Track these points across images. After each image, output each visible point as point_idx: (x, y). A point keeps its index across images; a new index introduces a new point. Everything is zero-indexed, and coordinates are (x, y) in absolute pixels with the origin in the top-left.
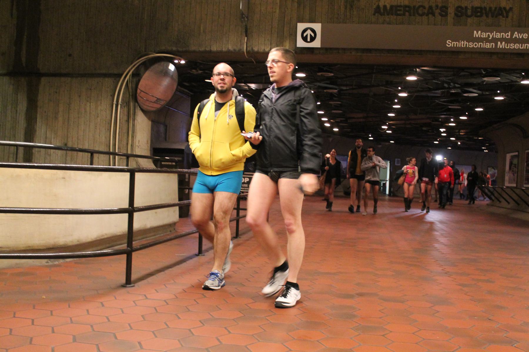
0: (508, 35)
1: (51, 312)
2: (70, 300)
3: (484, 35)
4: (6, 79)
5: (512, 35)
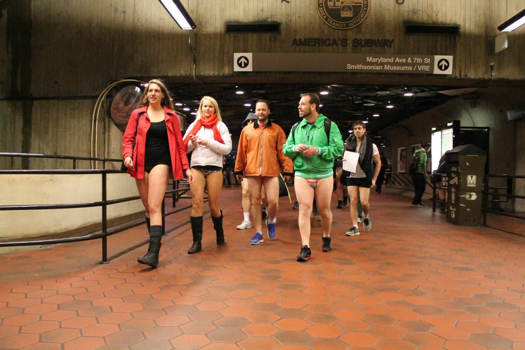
0: (391, 60)
1: (42, 286)
2: (57, 277)
3: (375, 60)
4: (5, 103)
5: (395, 60)
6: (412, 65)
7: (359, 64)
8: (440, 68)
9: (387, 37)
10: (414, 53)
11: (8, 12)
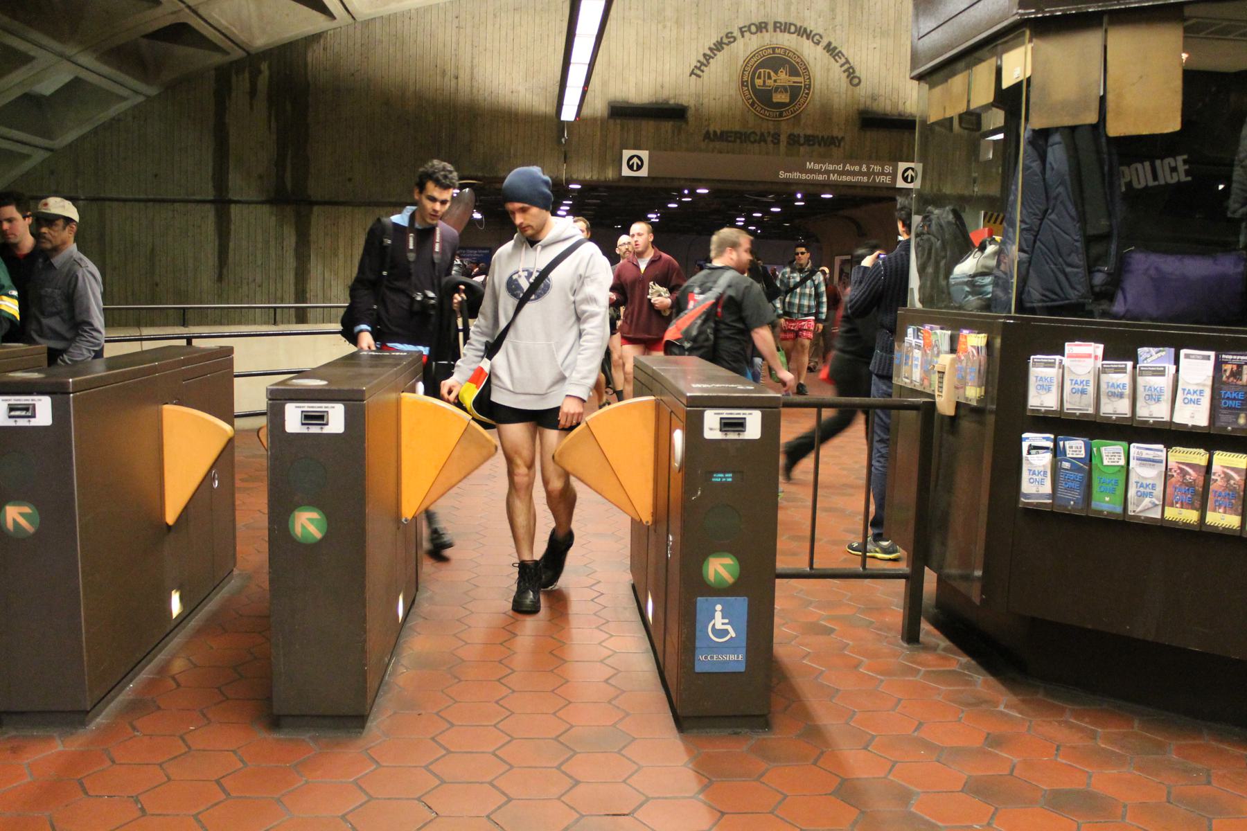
0: (840, 167)
3: (817, 167)
4: (266, 208)
6: (868, 174)
7: (796, 171)
8: (905, 179)
9: (836, 132)
10: (870, 158)
11: (270, 68)
